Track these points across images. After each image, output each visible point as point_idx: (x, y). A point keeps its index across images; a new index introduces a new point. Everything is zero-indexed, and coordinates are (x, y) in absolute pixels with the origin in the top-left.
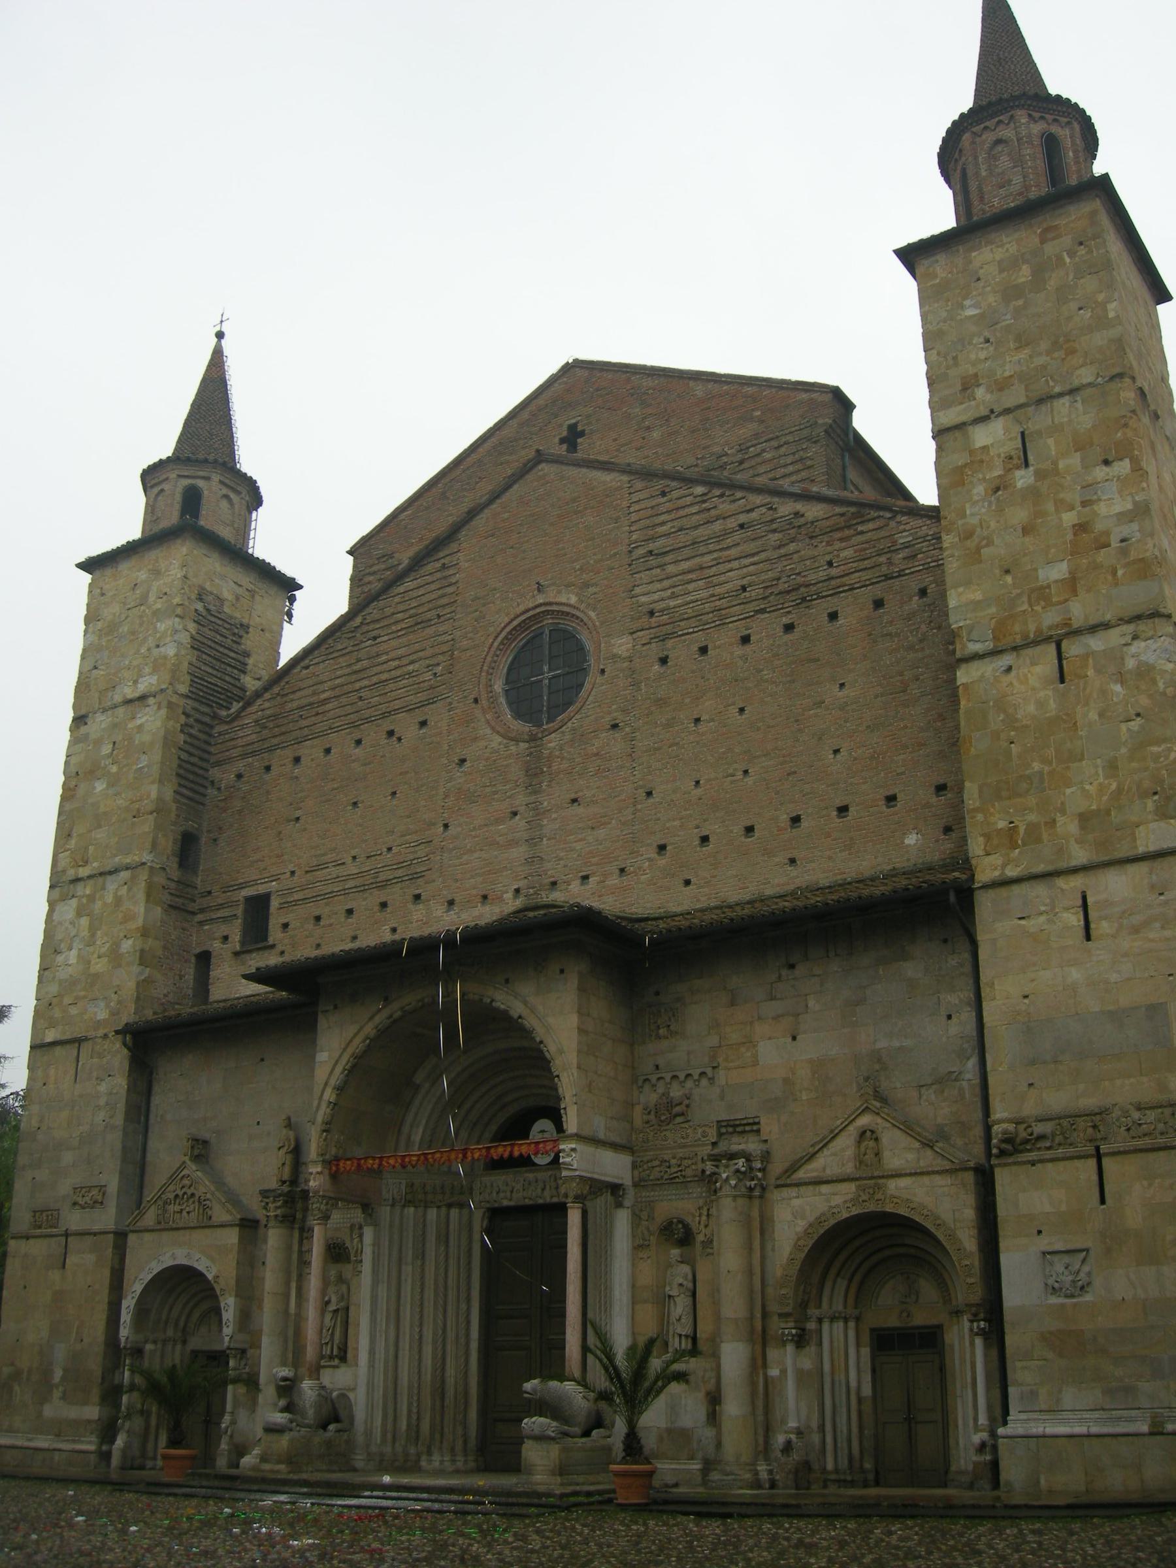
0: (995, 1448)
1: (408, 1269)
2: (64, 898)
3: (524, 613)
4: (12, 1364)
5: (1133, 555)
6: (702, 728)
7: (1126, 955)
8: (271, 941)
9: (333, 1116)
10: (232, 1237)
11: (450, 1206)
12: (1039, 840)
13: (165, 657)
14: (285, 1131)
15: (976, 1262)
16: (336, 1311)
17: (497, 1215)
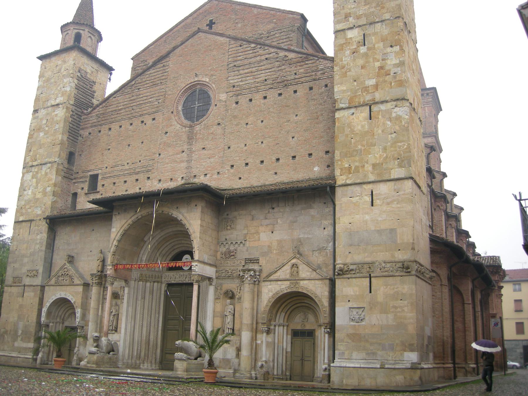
0: (329, 370)
1: (139, 302)
2: (28, 172)
3: (190, 83)
4: (4, 328)
5: (398, 79)
6: (248, 126)
7: (384, 212)
8: (98, 190)
9: (116, 250)
10: (80, 289)
11: (154, 282)
12: (358, 172)
13: (66, 91)
14: (100, 254)
15: (327, 309)
16: (114, 315)
17: (170, 285)
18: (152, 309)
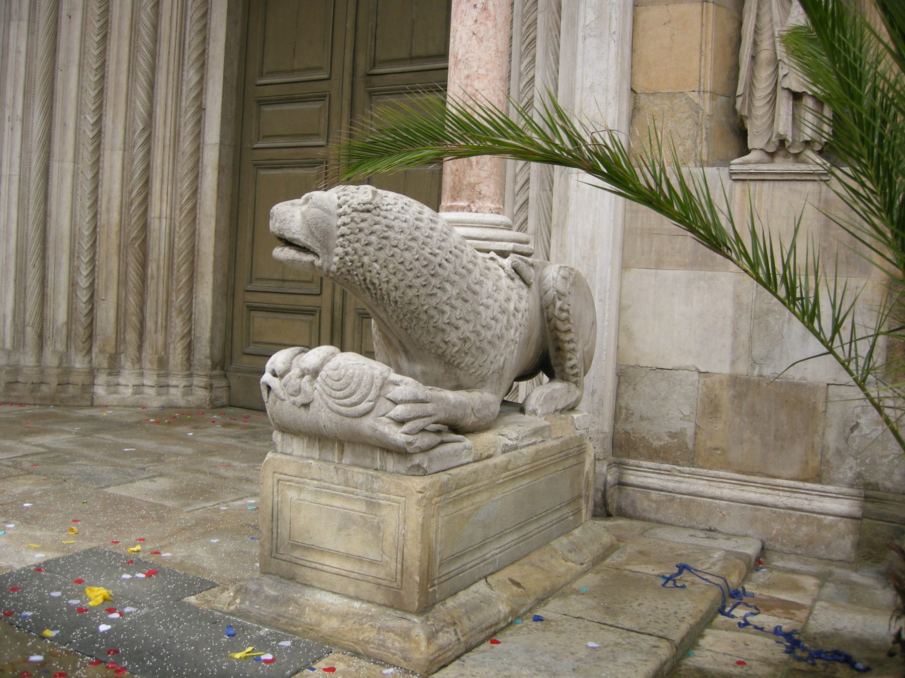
18: (155, 39)
